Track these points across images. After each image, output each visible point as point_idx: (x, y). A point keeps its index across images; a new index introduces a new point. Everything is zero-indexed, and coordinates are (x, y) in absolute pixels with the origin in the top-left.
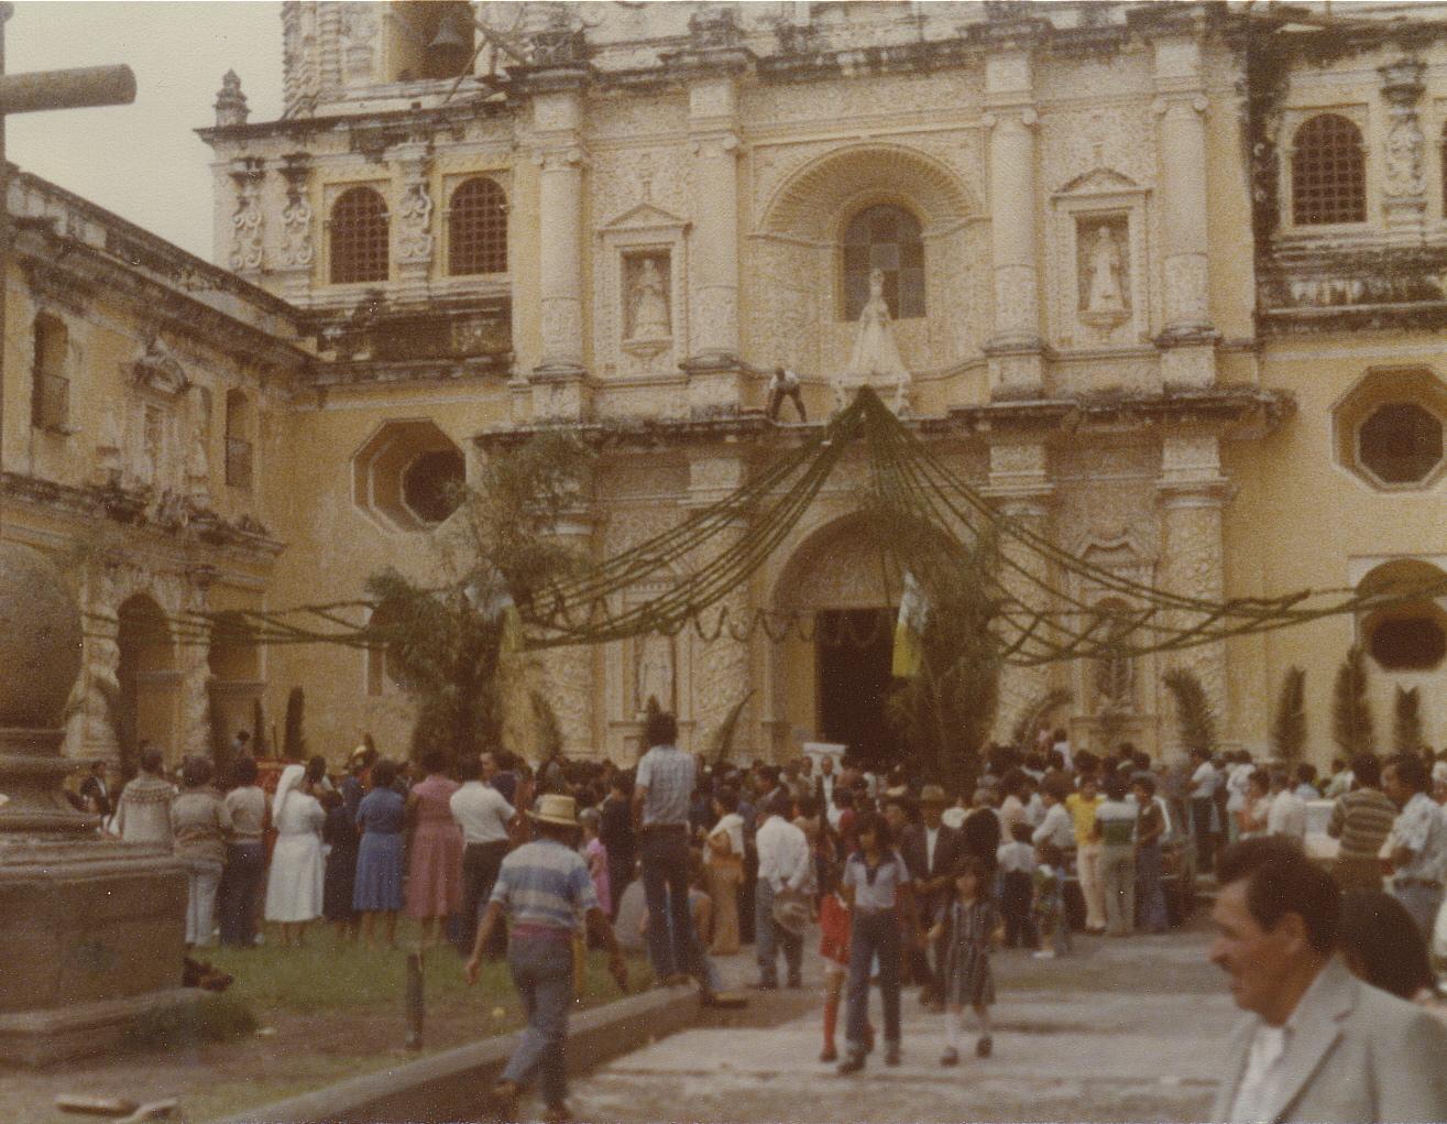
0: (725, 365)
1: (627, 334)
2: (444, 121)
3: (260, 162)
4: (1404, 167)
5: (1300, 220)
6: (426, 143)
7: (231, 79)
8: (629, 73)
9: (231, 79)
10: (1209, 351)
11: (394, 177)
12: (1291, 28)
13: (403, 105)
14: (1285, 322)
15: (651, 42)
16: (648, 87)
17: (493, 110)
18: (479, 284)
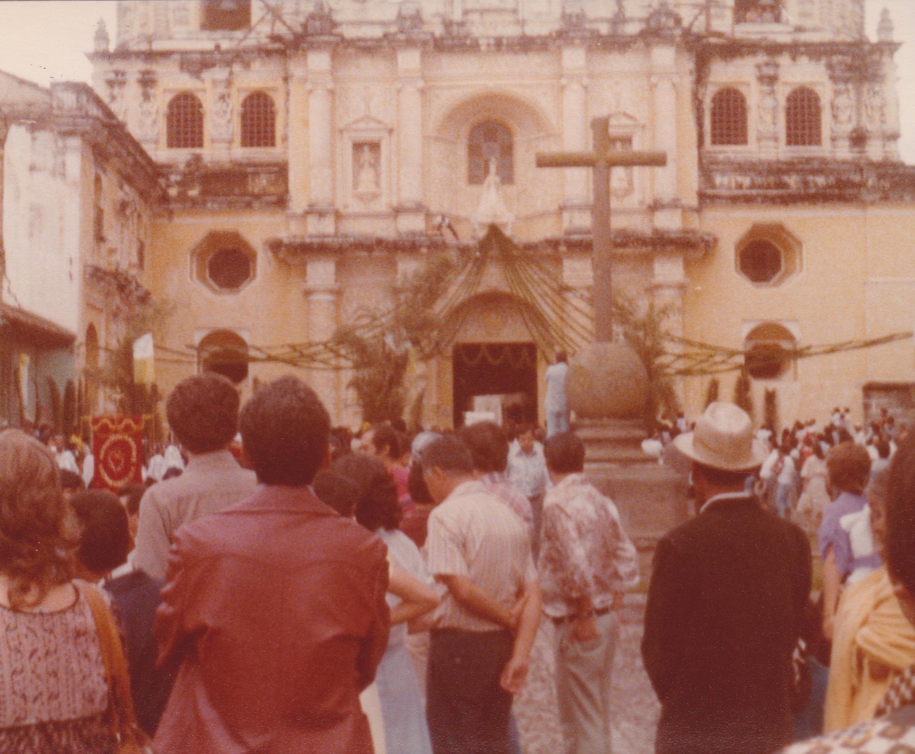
0: (419, 208)
1: (356, 185)
2: (240, 57)
3: (123, 74)
4: (768, 118)
5: (714, 142)
6: (227, 70)
7: (101, 23)
8: (359, 40)
9: (101, 23)
10: (679, 211)
11: (207, 89)
12: (713, 40)
13: (209, 46)
14: (713, 198)
15: (372, 23)
16: (368, 48)
17: (268, 53)
18: (260, 154)
